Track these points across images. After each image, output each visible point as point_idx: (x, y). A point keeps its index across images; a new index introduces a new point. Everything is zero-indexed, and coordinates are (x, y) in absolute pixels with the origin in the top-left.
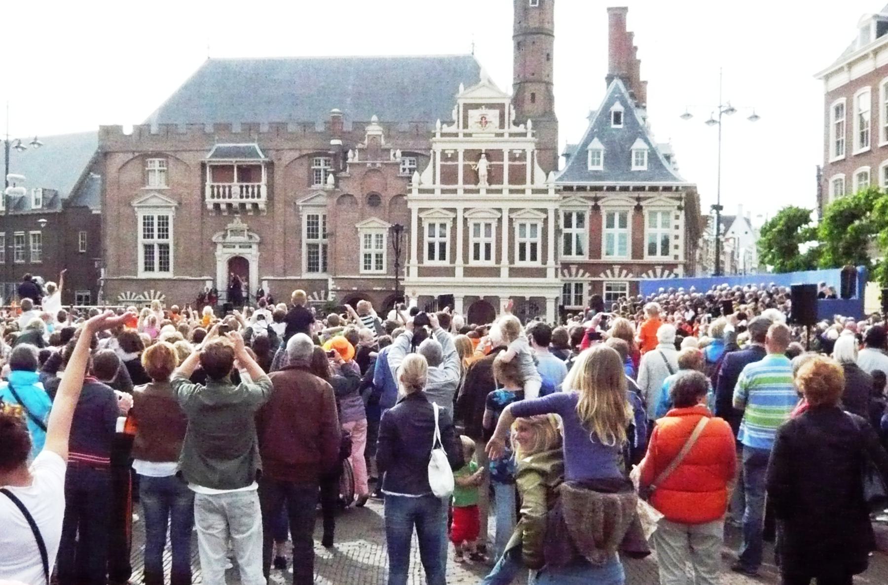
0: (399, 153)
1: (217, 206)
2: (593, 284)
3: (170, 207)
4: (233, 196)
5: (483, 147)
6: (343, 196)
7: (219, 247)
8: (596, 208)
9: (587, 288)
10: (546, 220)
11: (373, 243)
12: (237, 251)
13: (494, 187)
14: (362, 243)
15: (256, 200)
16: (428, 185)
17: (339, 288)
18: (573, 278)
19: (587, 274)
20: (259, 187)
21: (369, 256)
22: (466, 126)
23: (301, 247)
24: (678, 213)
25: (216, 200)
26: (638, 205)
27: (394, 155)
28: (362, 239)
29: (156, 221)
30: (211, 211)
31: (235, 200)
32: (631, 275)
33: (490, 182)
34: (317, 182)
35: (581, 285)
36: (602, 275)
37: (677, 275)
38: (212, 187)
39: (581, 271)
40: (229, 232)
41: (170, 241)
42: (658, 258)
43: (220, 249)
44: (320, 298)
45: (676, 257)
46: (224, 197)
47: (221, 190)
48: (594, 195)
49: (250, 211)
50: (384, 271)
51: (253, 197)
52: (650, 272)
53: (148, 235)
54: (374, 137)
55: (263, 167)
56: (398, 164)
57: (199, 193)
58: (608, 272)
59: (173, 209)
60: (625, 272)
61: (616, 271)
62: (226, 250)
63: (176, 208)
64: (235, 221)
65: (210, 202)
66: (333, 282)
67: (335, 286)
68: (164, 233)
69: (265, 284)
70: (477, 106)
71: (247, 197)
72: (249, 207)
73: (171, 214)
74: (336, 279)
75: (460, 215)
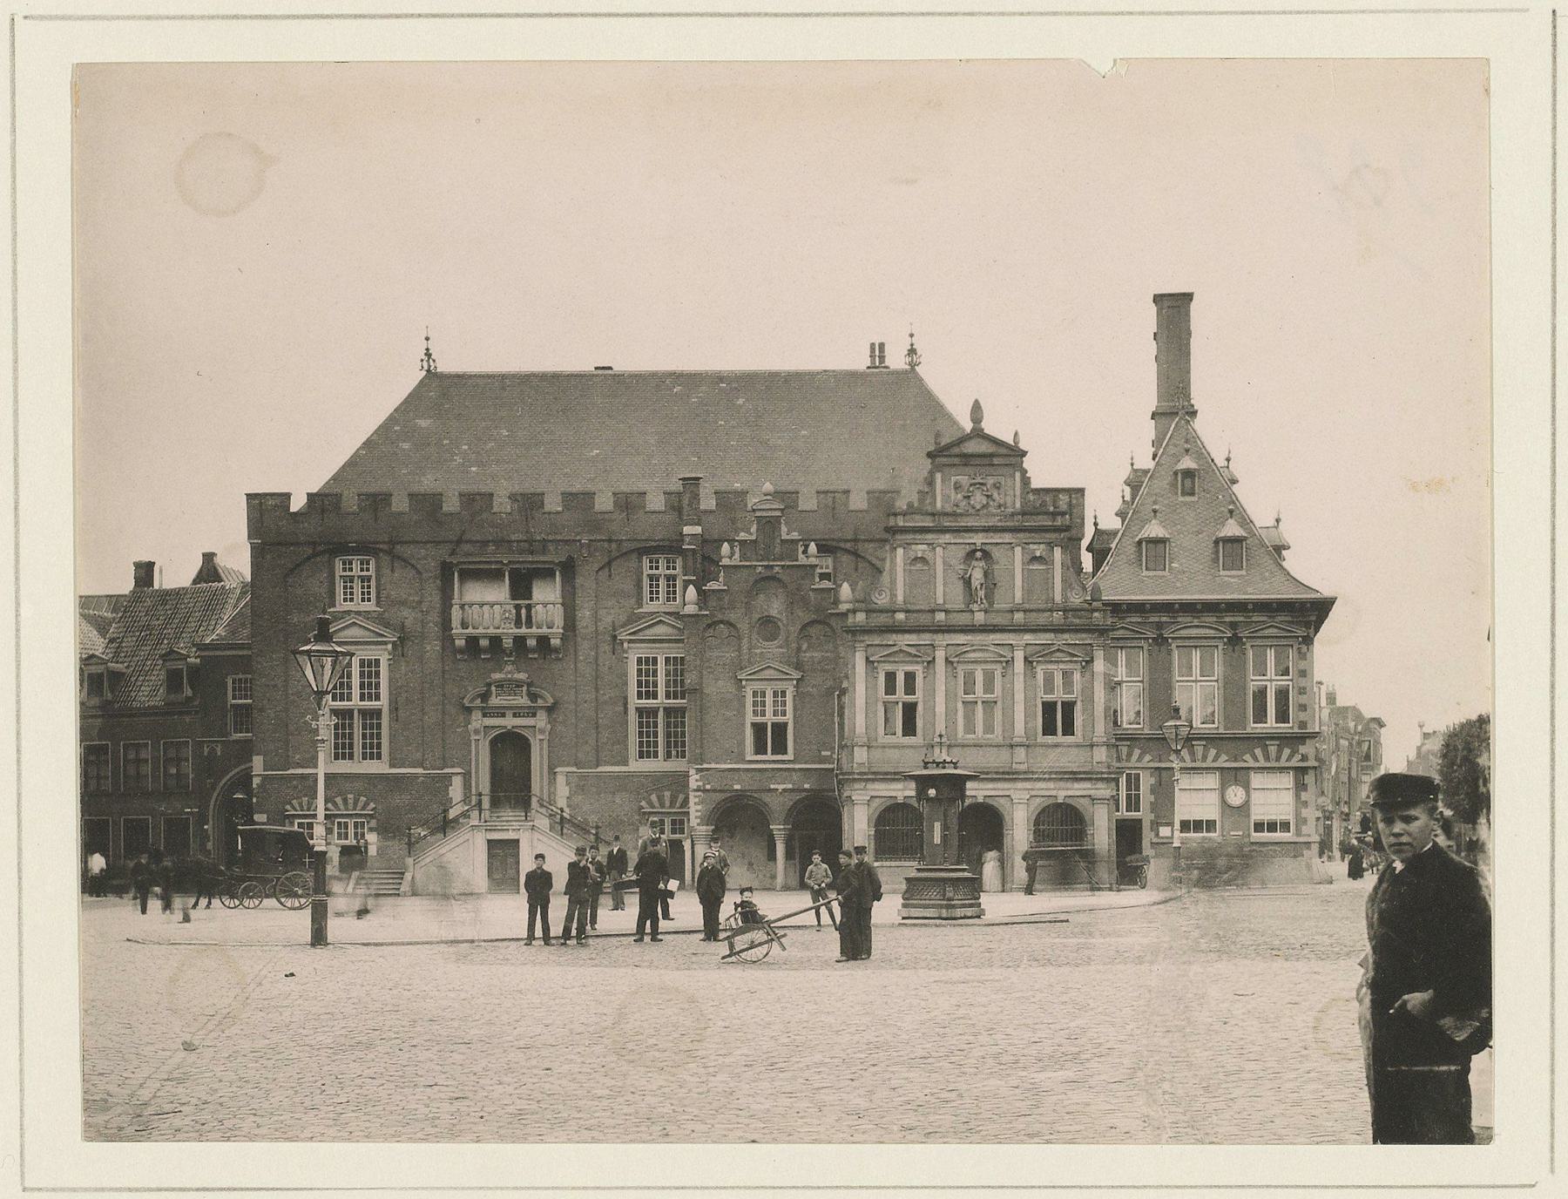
0: (813, 548)
3: (385, 643)
5: (979, 539)
7: (476, 715)
9: (1146, 782)
11: (769, 709)
12: (509, 722)
14: (749, 708)
15: (545, 630)
17: (708, 787)
18: (1124, 764)
21: (759, 729)
23: (626, 712)
25: (470, 630)
26: (1235, 635)
27: (805, 552)
28: (749, 700)
30: (461, 651)
31: (505, 631)
32: (1224, 757)
34: (652, 599)
37: (1304, 758)
39: (1137, 752)
40: (493, 688)
41: (383, 703)
42: (1271, 724)
43: (477, 721)
44: (662, 806)
45: (1303, 725)
48: (1157, 619)
49: (533, 651)
50: (790, 756)
52: (1258, 752)
55: (558, 573)
56: (814, 567)
57: (434, 617)
59: (390, 646)
60: (1213, 752)
63: (394, 643)
64: (509, 668)
66: (697, 777)
67: (700, 783)
68: (370, 690)
69: (561, 779)
71: (529, 624)
72: (532, 643)
74: (701, 770)
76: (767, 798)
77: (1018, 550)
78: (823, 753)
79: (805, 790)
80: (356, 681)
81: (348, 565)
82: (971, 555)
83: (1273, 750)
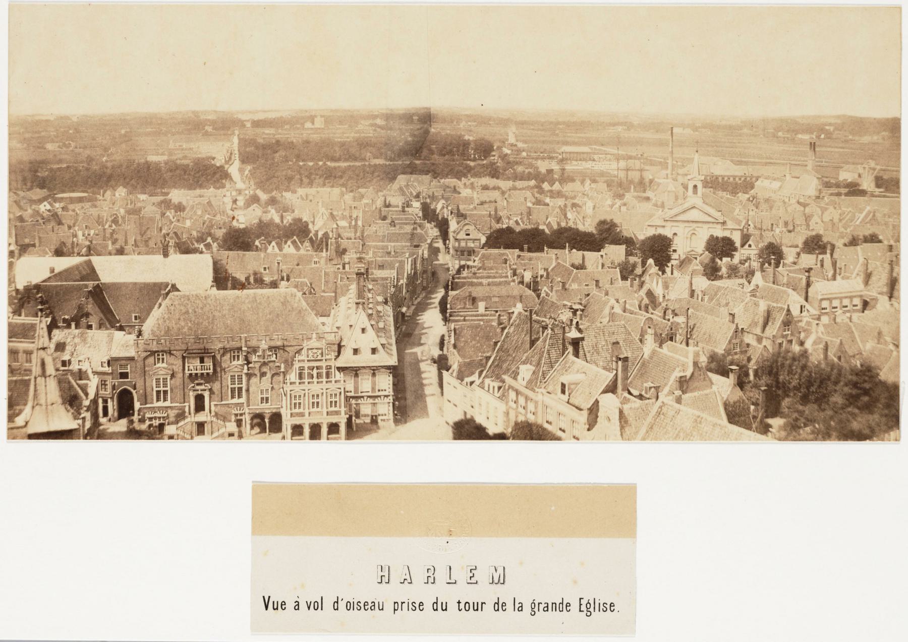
1: (191, 374)
10: (340, 393)
12: (200, 392)
13: (320, 380)
15: (208, 371)
16: (293, 380)
22: (308, 356)
25: (190, 372)
33: (318, 378)
41: (168, 389)
53: (158, 385)
54: (264, 351)
68: (165, 385)
70: (312, 349)
73: (169, 378)
75: (306, 392)
81: (158, 355)
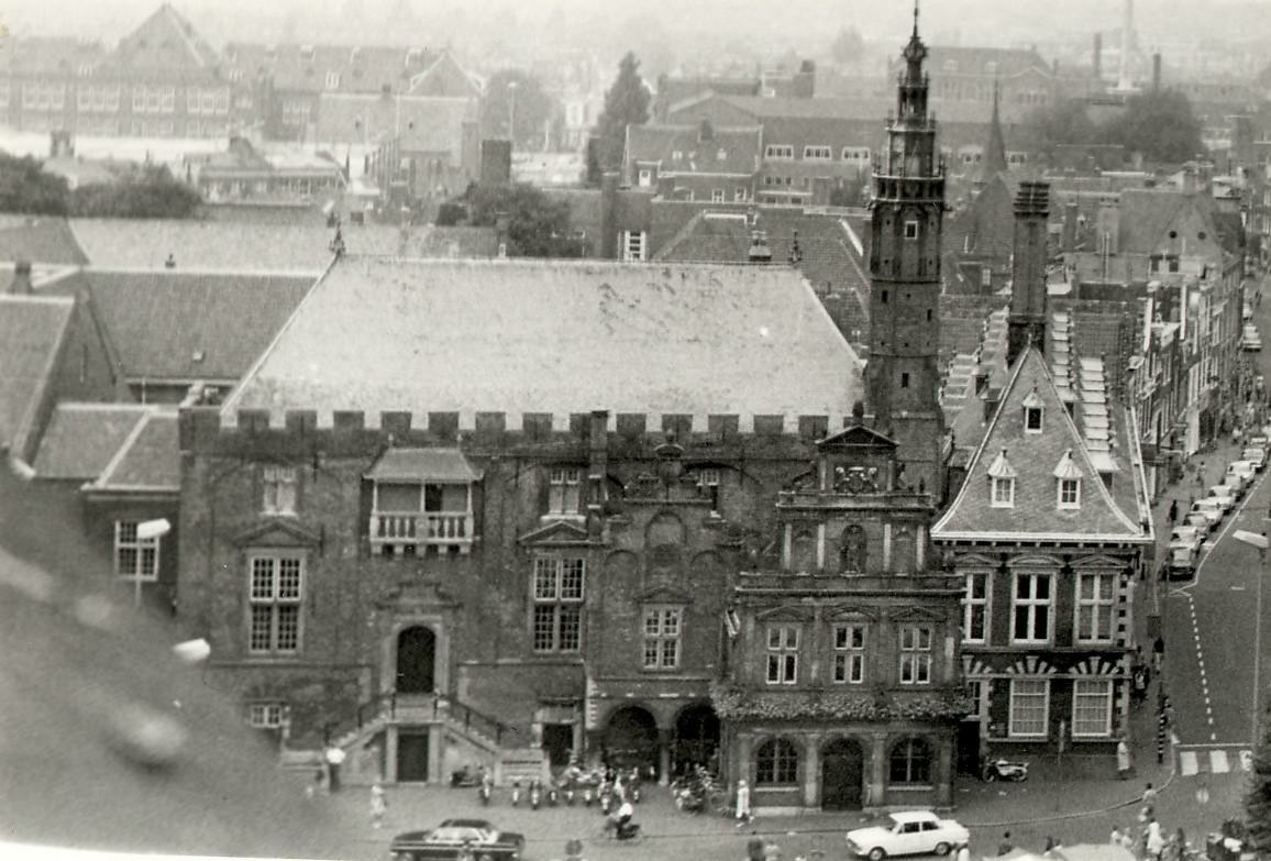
2: (996, 682)
4: (417, 533)
6: (617, 552)
8: (1003, 570)
12: (420, 618)
15: (456, 540)
17: (604, 695)
19: (988, 669)
20: (462, 520)
24: (1125, 577)
25: (388, 539)
29: (277, 568)
30: (377, 555)
35: (978, 684)
36: (1010, 669)
38: (382, 520)
46: (402, 534)
47: (397, 522)
51: (451, 534)
57: (352, 522)
58: (1019, 665)
61: (1031, 664)
62: (397, 617)
65: (375, 539)
66: (595, 686)
68: (289, 586)
71: (441, 534)
76: (654, 704)
77: (888, 527)
78: (709, 666)
79: (691, 699)
80: (276, 578)
82: (848, 530)
83: (1095, 662)
